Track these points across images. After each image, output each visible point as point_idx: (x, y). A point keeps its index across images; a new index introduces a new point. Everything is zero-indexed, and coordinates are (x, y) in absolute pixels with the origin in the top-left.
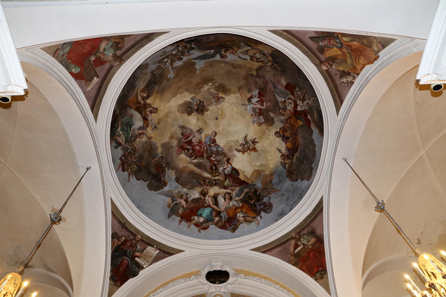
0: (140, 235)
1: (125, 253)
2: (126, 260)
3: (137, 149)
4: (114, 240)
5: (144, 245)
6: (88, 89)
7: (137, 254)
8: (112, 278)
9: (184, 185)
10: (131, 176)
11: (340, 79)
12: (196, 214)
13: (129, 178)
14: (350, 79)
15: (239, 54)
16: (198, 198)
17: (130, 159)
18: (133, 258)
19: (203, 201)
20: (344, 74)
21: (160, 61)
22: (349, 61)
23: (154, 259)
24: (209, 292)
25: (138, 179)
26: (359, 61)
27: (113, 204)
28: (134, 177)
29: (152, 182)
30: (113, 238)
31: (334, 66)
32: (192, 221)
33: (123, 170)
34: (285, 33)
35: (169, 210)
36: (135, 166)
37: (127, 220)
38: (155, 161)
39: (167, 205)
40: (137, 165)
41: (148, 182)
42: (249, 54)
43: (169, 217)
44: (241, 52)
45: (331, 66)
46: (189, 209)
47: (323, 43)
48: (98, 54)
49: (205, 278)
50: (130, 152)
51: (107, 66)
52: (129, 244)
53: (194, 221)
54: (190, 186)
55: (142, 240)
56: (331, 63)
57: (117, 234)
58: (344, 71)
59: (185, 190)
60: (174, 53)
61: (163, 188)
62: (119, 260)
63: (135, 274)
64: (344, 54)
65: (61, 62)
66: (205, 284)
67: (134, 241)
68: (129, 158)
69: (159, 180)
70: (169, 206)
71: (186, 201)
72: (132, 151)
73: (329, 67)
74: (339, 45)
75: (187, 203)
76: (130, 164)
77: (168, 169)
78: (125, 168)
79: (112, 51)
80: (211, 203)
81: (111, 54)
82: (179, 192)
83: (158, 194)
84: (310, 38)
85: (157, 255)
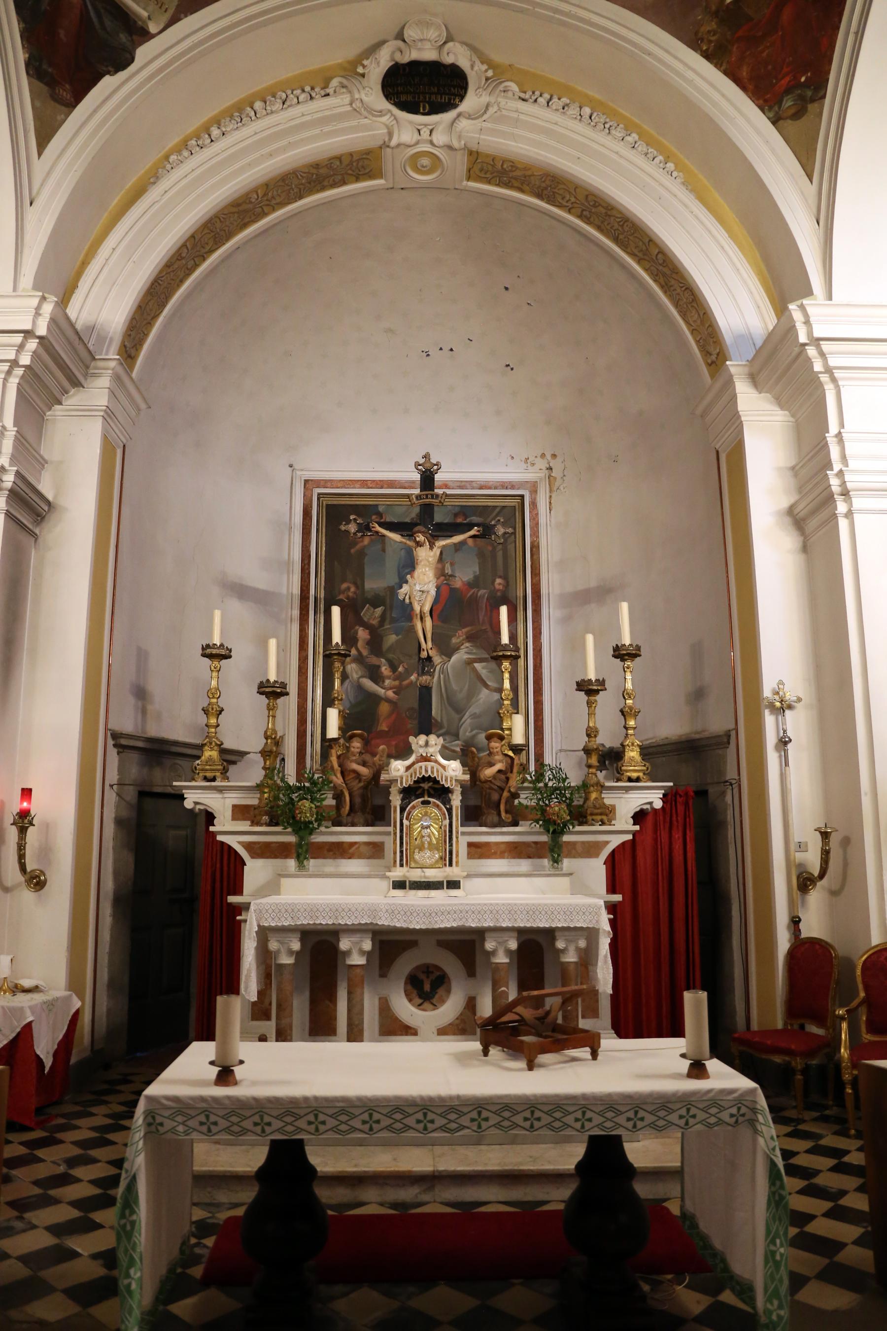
24: (393, 143)
49: (379, 87)
66: (381, 114)
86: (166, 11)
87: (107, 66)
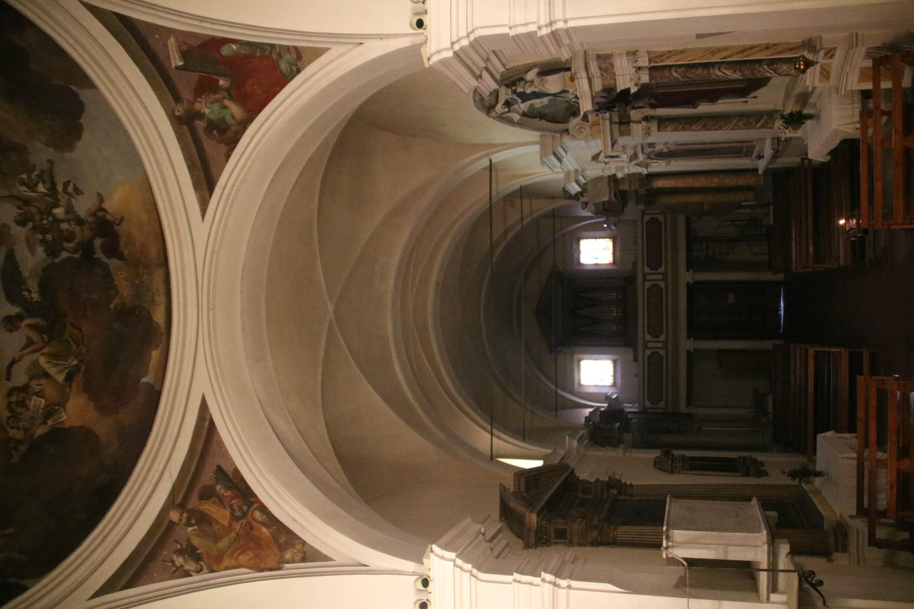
6: (172, 41)
11: (175, 553)
14: (190, 566)
15: (28, 360)
20: (191, 552)
21: (49, 177)
22: (223, 543)
26: (239, 554)
31: (190, 529)
34: (207, 424)
42: (34, 384)
44: (36, 363)
45: (188, 524)
47: (222, 491)
48: (226, 94)
51: (186, 94)
56: (193, 522)
58: (194, 549)
60: (59, 212)
64: (230, 529)
65: (273, 46)
73: (184, 521)
74: (239, 514)
79: (213, 117)
81: (207, 111)
84: (219, 469)
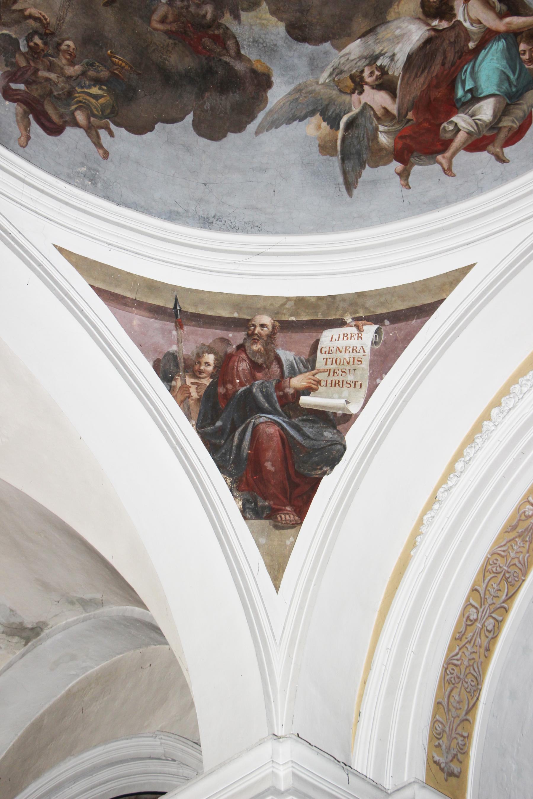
0: (264, 310)
1: (249, 405)
2: (269, 424)
3: (50, 19)
4: (178, 383)
5: (304, 339)
7: (298, 382)
8: (251, 511)
9: (337, 33)
10: (103, 133)
12: (453, 106)
13: (98, 144)
16: (428, 41)
17: (53, 76)
18: (289, 403)
19: (453, 34)
23: (372, 364)
25: (140, 128)
27: (84, 265)
28: (120, 132)
29: (207, 106)
30: (167, 378)
32: (451, 141)
33: (54, 130)
35: (336, 162)
36: (95, 90)
37: (174, 288)
38: (163, 20)
39: (316, 149)
40: (97, 81)
41: (190, 118)
43: (350, 186)
46: (415, 106)
50: (34, 50)
52: (244, 366)
53: (461, 137)
54: (366, 15)
55: (286, 326)
57: (173, 357)
59: (355, 48)
61: (265, 101)
62: (241, 440)
63: (332, 455)
67: (256, 347)
68: (43, 73)
69: (230, 82)
70: (326, 148)
71: (385, 84)
72: (37, 40)
75: (393, 94)
76: (70, 94)
77: (237, 17)
78: (55, 117)
80: (491, 21)
82: (337, 71)
83: (257, 133)
85: (375, 343)
86: (361, 387)
87: (321, 469)
